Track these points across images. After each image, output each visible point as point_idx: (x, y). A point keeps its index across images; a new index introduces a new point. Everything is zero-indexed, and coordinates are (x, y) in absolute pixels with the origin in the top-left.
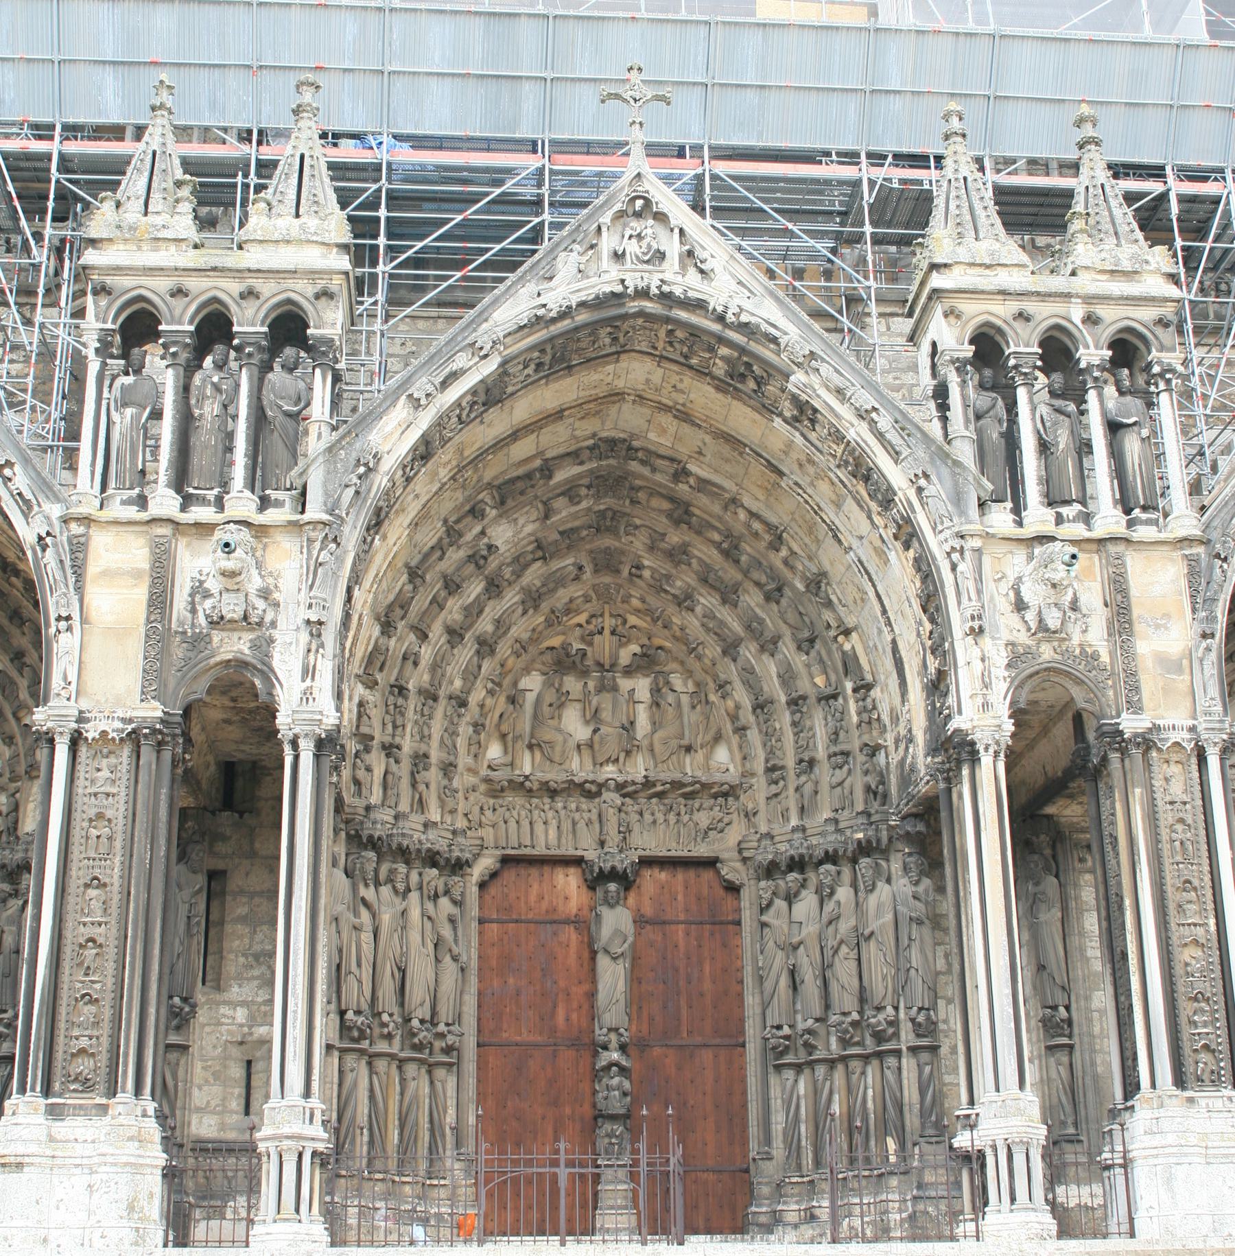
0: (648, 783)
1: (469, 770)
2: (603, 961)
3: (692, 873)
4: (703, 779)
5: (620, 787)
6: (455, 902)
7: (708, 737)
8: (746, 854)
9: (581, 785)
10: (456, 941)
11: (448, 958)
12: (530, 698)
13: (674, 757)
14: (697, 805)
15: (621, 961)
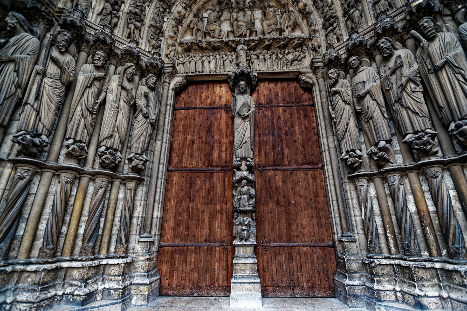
0: (261, 40)
1: (172, 37)
2: (238, 121)
3: (285, 84)
4: (289, 37)
5: (247, 43)
6: (152, 89)
7: (290, 23)
8: (316, 65)
9: (227, 43)
10: (148, 106)
11: (140, 116)
12: (206, 19)
13: (273, 33)
14: (286, 52)
15: (248, 119)
